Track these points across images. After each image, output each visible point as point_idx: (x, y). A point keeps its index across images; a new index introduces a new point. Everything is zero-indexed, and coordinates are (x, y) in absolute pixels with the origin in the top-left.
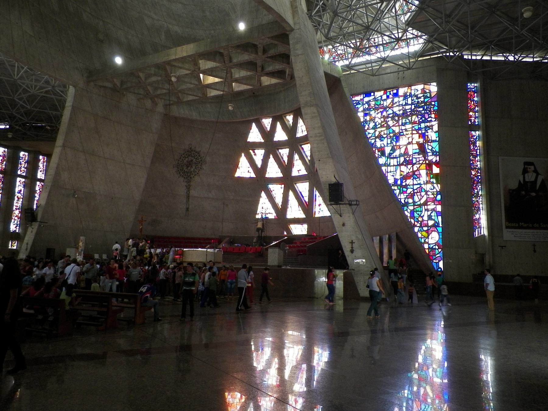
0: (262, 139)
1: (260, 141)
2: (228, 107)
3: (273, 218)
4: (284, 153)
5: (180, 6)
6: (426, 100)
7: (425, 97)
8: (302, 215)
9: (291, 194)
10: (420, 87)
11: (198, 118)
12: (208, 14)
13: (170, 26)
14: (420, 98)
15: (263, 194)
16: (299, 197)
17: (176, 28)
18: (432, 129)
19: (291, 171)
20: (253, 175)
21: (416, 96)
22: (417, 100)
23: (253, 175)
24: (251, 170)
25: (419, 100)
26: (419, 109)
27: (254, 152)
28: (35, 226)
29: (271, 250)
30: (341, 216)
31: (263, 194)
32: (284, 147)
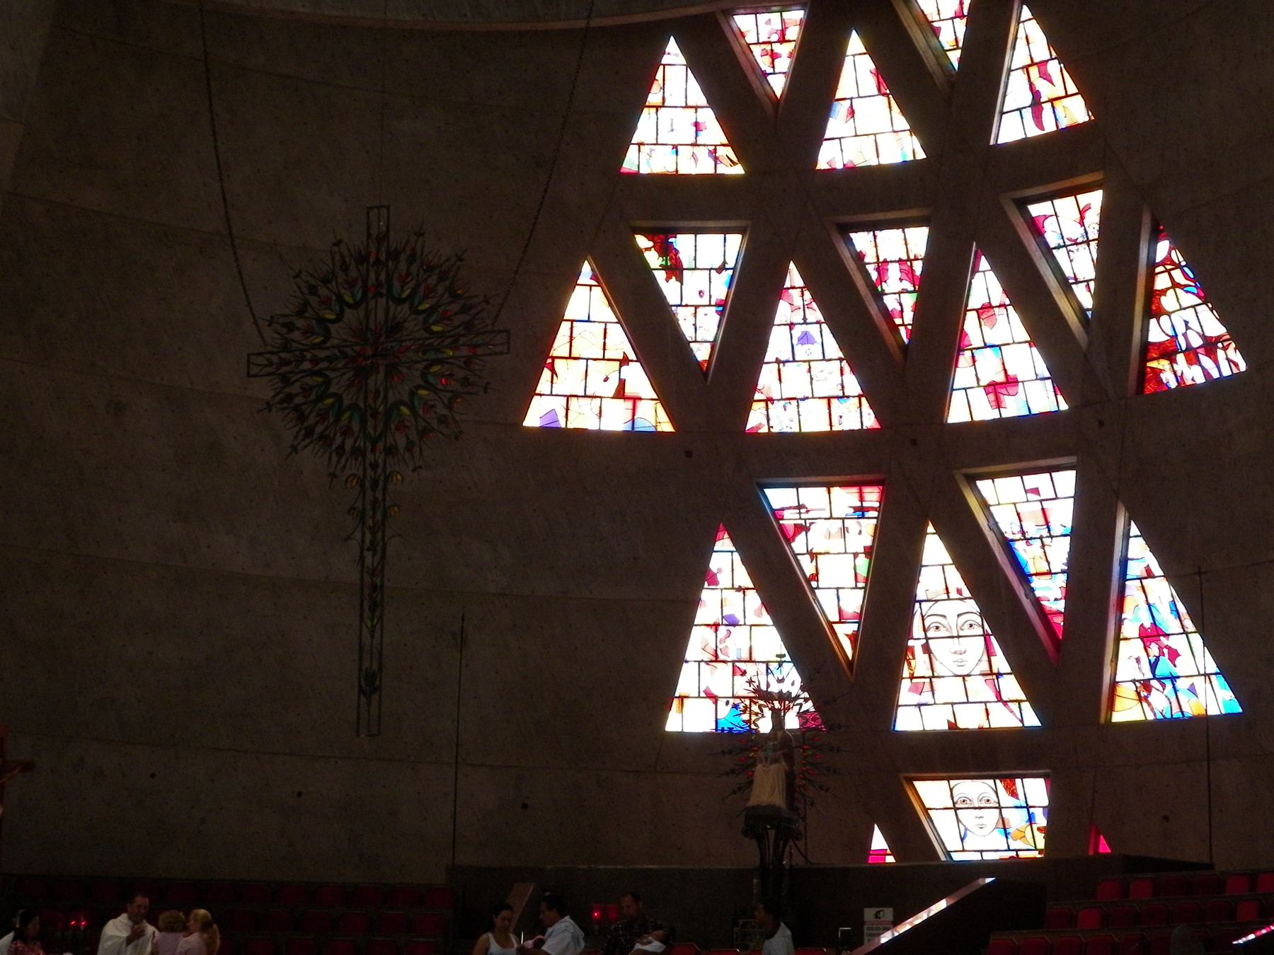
1: (705, 167)
19: (941, 391)
20: (654, 417)
23: (654, 417)
24: (638, 380)
27: (666, 250)
32: (890, 215)
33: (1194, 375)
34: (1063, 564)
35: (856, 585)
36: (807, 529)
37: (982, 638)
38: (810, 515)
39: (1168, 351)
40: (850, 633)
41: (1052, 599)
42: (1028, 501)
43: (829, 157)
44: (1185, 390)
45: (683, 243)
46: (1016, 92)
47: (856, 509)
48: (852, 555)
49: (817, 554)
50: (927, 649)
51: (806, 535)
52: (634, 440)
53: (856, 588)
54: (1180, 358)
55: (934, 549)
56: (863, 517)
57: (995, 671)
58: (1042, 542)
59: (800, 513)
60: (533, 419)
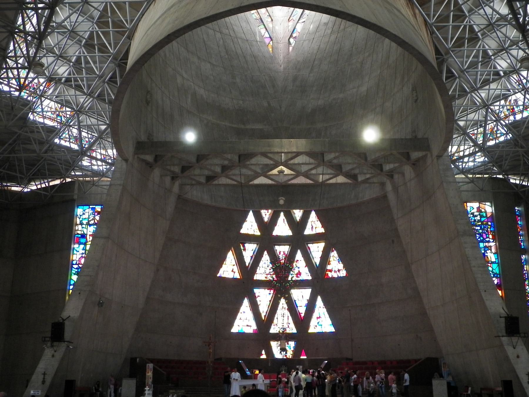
0: (258, 231)
2: (279, 201)
3: (251, 331)
4: (282, 250)
5: (208, 66)
6: (483, 219)
7: (481, 216)
8: (292, 329)
9: (283, 302)
10: (476, 205)
11: (209, 203)
12: (238, 80)
13: (197, 88)
14: (476, 216)
15: (246, 302)
16: (292, 307)
17: (202, 92)
18: (491, 250)
21: (473, 214)
22: (473, 218)
24: (236, 269)
25: (476, 218)
26: (477, 228)
27: (244, 246)
28: (62, 348)
29: (437, 381)
30: (514, 348)
31: (246, 302)
32: (284, 244)
33: (335, 275)
39: (331, 271)
43: (275, 233)
44: (333, 278)
45: (247, 245)
46: (309, 226)
50: (277, 318)
52: (234, 279)
54: (333, 272)
55: (283, 301)
60: (218, 275)
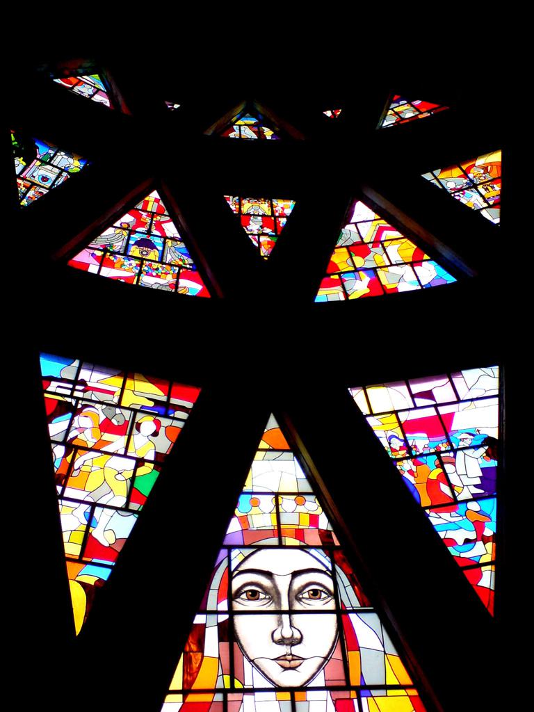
34: (476, 486)
35: (127, 503)
36: (76, 412)
37: (333, 617)
38: (88, 395)
40: (91, 581)
41: (460, 542)
42: (416, 408)
47: (157, 402)
48: (134, 462)
49: (78, 448)
50: (228, 633)
51: (72, 420)
53: (126, 509)
56: (166, 416)
57: (355, 681)
58: (440, 458)
59: (73, 390)
